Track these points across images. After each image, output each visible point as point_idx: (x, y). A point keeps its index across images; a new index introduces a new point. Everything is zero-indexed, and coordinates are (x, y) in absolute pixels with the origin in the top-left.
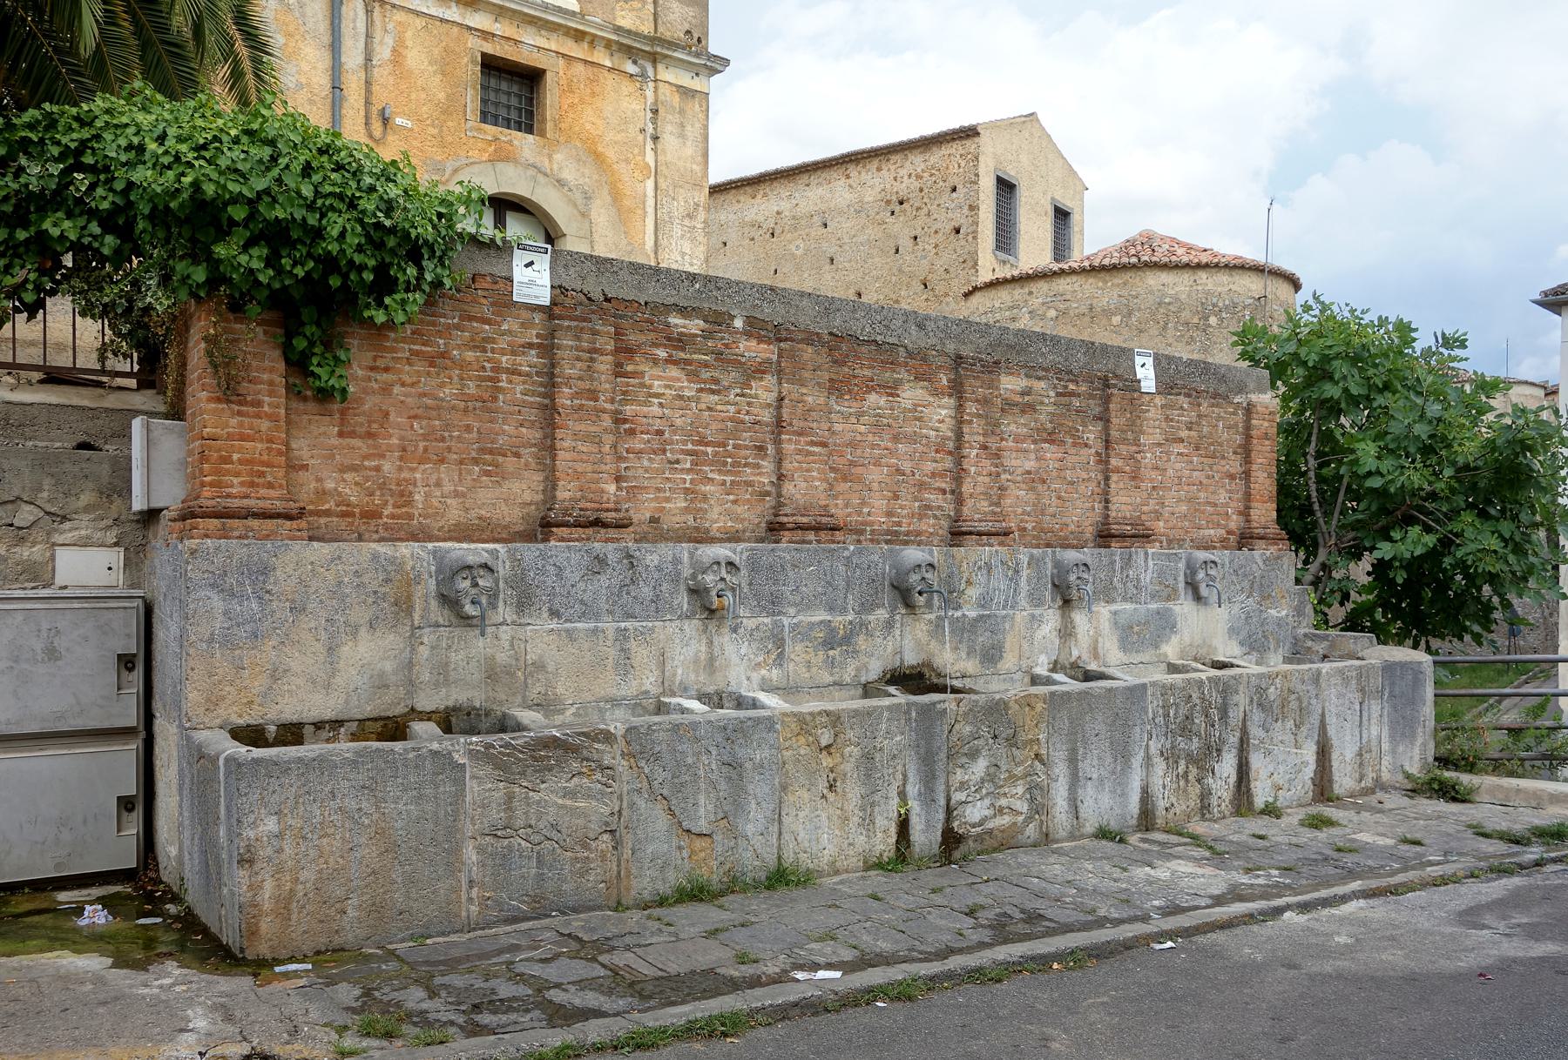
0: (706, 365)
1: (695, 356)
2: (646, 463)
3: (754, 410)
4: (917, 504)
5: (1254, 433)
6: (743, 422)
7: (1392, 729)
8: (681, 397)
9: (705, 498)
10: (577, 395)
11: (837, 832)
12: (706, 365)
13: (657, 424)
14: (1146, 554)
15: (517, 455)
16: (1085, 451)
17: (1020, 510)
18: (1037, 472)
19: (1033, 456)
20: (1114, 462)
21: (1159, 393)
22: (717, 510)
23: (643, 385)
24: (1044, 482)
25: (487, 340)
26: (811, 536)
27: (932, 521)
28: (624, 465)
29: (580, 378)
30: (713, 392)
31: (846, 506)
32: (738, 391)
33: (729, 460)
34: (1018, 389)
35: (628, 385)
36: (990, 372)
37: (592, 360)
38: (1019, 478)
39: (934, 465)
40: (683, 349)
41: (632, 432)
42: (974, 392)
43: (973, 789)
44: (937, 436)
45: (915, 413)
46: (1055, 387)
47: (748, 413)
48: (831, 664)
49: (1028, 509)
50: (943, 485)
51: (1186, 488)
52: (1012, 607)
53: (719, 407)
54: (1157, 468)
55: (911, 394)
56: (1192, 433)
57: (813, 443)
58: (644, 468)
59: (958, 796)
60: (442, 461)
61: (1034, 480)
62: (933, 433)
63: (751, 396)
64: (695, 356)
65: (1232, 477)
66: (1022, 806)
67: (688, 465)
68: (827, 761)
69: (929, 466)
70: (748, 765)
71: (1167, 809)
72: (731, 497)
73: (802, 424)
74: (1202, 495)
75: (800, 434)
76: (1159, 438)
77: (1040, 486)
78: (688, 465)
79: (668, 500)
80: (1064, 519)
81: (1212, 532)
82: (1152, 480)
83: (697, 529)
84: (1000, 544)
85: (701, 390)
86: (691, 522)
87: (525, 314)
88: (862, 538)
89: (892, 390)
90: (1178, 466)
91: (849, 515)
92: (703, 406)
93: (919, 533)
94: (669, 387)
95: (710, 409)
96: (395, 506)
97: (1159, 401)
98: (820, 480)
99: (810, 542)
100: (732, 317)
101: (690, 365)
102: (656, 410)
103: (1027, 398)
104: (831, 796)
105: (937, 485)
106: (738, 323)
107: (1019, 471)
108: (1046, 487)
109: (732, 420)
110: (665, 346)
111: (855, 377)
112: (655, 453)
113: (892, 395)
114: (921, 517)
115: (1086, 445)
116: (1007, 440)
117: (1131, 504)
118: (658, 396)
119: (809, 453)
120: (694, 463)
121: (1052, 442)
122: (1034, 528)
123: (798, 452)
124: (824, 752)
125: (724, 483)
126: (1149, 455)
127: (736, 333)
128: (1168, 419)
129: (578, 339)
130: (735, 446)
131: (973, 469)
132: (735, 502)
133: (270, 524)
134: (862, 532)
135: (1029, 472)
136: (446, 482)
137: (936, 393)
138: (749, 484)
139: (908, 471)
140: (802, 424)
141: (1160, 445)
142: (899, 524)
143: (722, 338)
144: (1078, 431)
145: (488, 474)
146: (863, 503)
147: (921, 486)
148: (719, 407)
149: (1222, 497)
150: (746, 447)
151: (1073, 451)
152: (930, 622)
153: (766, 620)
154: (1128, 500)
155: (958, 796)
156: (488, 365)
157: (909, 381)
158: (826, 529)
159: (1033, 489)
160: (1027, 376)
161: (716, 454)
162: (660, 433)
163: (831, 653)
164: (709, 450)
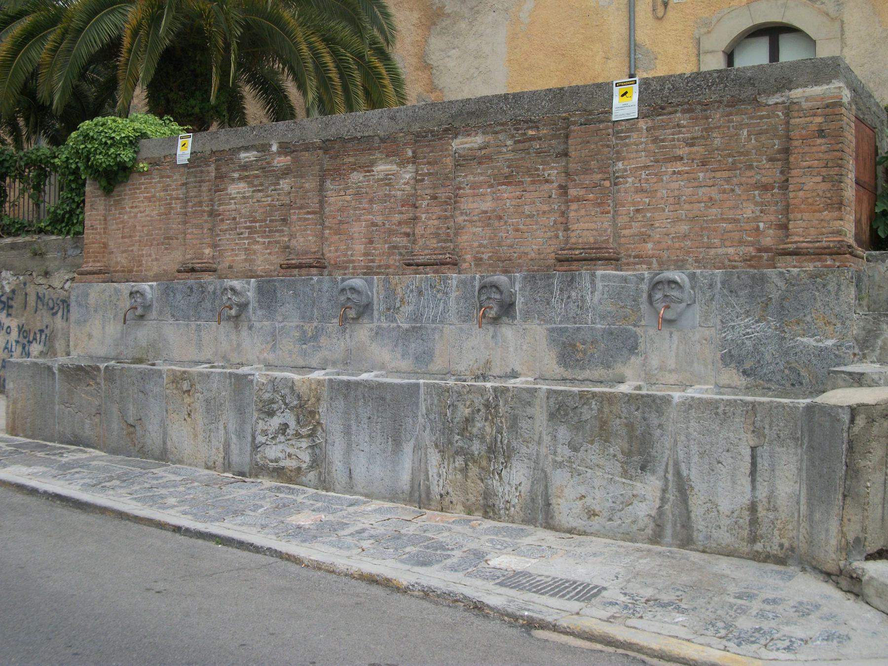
0: (257, 176)
1: (252, 173)
2: (228, 236)
3: (282, 198)
4: (386, 246)
5: (794, 134)
6: (275, 206)
7: (810, 489)
8: (244, 197)
9: (255, 253)
10: (194, 206)
11: (192, 442)
12: (257, 176)
13: (234, 214)
14: (593, 275)
15: (177, 239)
16: (546, 187)
17: (476, 244)
18: (494, 211)
19: (489, 198)
20: (573, 192)
21: (642, 115)
22: (261, 258)
23: (227, 194)
24: (500, 218)
25: (168, 185)
26: (296, 271)
27: (398, 257)
28: (218, 238)
29: (196, 197)
30: (260, 191)
31: (336, 251)
32: (273, 187)
33: (267, 229)
34: (476, 146)
35: (221, 195)
36: (440, 139)
37: (200, 186)
38: (475, 218)
39: (402, 216)
40: (246, 170)
41: (222, 220)
42: (425, 158)
43: (270, 436)
44: (402, 195)
45: (387, 181)
46: (513, 136)
47: (278, 200)
48: (304, 354)
49: (485, 242)
50: (408, 230)
51: (686, 206)
52: (441, 322)
53: (263, 199)
54: (642, 191)
55: (382, 168)
56: (695, 149)
57: (308, 213)
58: (226, 240)
59: (261, 439)
60: (152, 245)
61: (488, 219)
62: (399, 193)
63: (280, 190)
64: (252, 173)
65: (765, 188)
66: (306, 457)
67: (247, 235)
68: (187, 400)
69: (397, 217)
70: (150, 394)
71: (441, 496)
72: (268, 251)
73: (302, 202)
74: (713, 211)
75: (300, 208)
76: (643, 159)
77: (496, 223)
78: (247, 235)
79: (236, 255)
80: (522, 249)
81: (731, 251)
82: (634, 203)
83: (251, 271)
84: (434, 272)
85: (254, 191)
86: (248, 268)
87: (182, 170)
88: (346, 272)
89: (367, 168)
90: (675, 185)
91: (338, 257)
92: (255, 200)
93: (388, 267)
94: (238, 193)
95: (258, 201)
96: (137, 267)
97: (642, 124)
98: (312, 235)
99: (295, 276)
100: (271, 146)
101: (249, 178)
102: (233, 207)
103: (483, 152)
104: (189, 420)
105: (403, 230)
106: (274, 148)
107: (476, 212)
108: (502, 222)
109: (269, 205)
110: (238, 171)
111: (344, 164)
112: (232, 230)
113: (369, 171)
114: (390, 254)
115: (547, 181)
116: (464, 189)
117: (596, 230)
118: (233, 199)
119: (308, 219)
120: (250, 233)
121: (509, 184)
122: (490, 258)
123: (300, 219)
124: (186, 395)
125: (264, 243)
126: (630, 180)
127: (273, 154)
128: (656, 140)
129: (196, 177)
130: (271, 221)
131: (424, 216)
132: (270, 254)
133: (91, 277)
134: (346, 268)
135: (486, 212)
136: (153, 255)
137: (402, 164)
138: (277, 242)
139: (380, 223)
140: (302, 202)
141: (646, 167)
142: (373, 261)
143: (266, 159)
144: (538, 169)
145: (166, 249)
146: (348, 248)
147: (391, 233)
148: (263, 199)
149: (749, 211)
150: (276, 221)
151: (532, 188)
152: (371, 330)
153: (267, 323)
154: (593, 226)
155: (261, 439)
156: (168, 197)
157: (381, 159)
158: (306, 267)
159: (489, 225)
160: (484, 133)
161: (260, 227)
162: (234, 219)
163: (304, 346)
164: (257, 224)
